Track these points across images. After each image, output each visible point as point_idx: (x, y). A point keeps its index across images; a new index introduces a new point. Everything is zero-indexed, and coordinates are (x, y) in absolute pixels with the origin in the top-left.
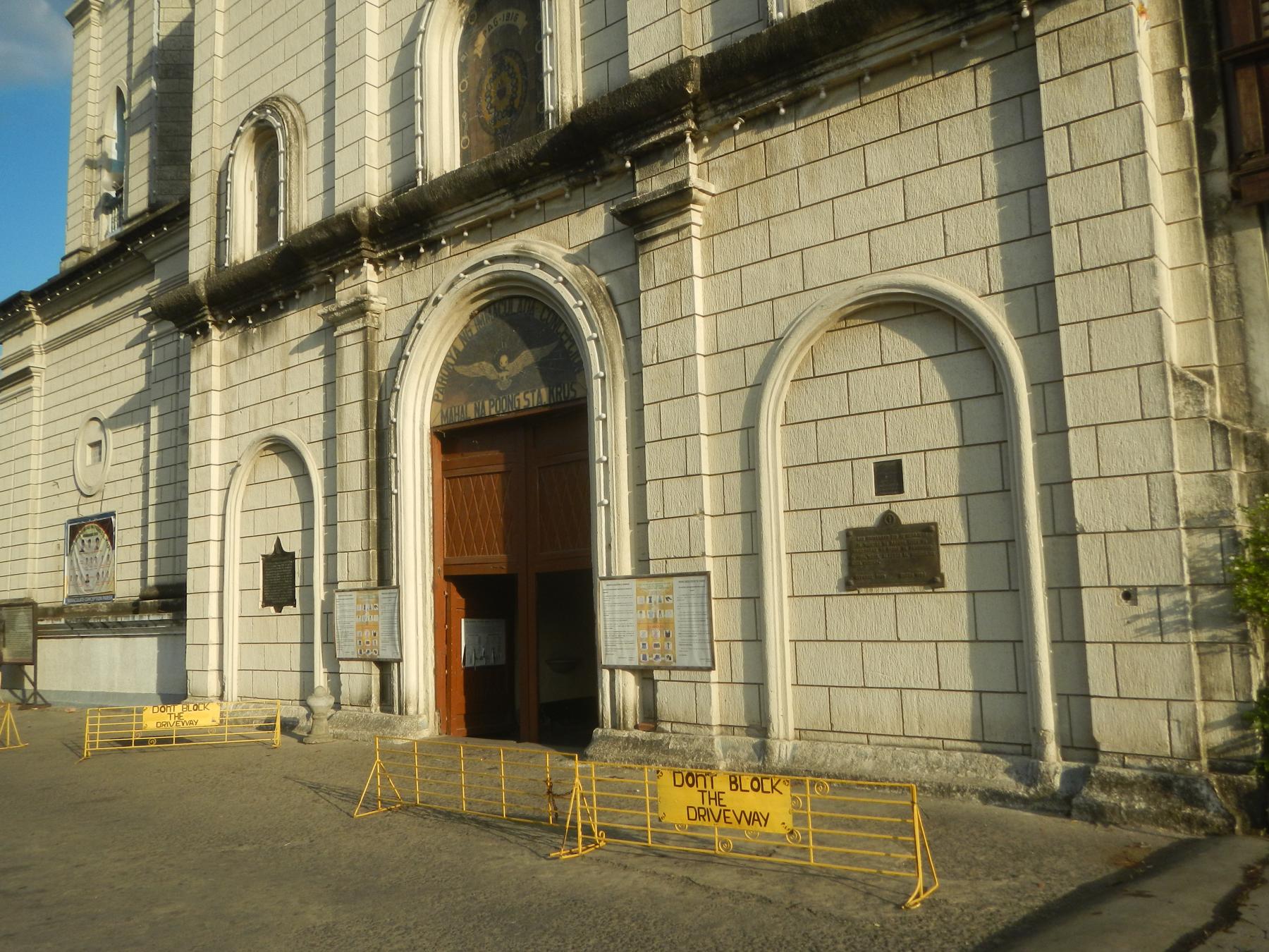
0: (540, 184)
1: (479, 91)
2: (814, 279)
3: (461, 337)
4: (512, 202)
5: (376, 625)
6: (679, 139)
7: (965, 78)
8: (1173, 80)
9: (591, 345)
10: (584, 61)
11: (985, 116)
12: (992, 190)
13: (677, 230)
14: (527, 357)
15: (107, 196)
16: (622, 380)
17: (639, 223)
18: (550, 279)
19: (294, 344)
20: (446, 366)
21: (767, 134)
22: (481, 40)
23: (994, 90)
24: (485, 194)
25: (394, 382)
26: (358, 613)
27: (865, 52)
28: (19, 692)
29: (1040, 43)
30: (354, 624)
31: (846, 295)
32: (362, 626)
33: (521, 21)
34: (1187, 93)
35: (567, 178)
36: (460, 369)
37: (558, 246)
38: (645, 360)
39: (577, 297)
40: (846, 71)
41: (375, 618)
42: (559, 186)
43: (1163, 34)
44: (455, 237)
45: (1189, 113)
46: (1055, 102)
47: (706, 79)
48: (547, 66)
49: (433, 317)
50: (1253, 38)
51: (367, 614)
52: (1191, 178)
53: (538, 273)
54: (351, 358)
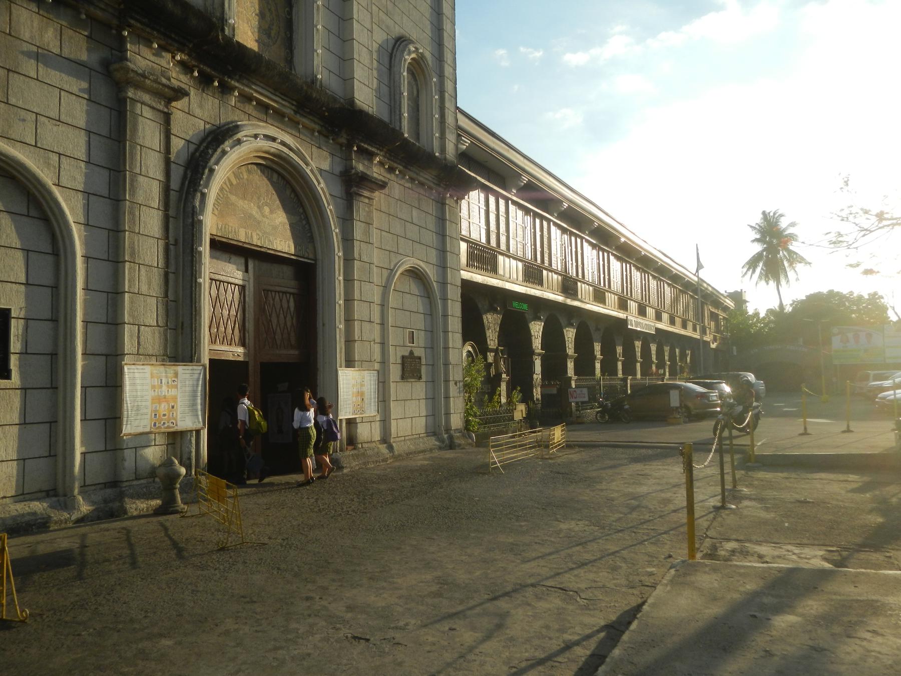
0: (311, 117)
4: (292, 113)
5: (175, 398)
13: (369, 198)
19: (35, 49)
24: (285, 95)
26: (153, 387)
27: (421, 174)
28: (591, 413)
30: (149, 398)
32: (158, 400)
35: (322, 126)
41: (173, 392)
42: (317, 127)
44: (246, 98)
51: (164, 388)
54: (147, 131)
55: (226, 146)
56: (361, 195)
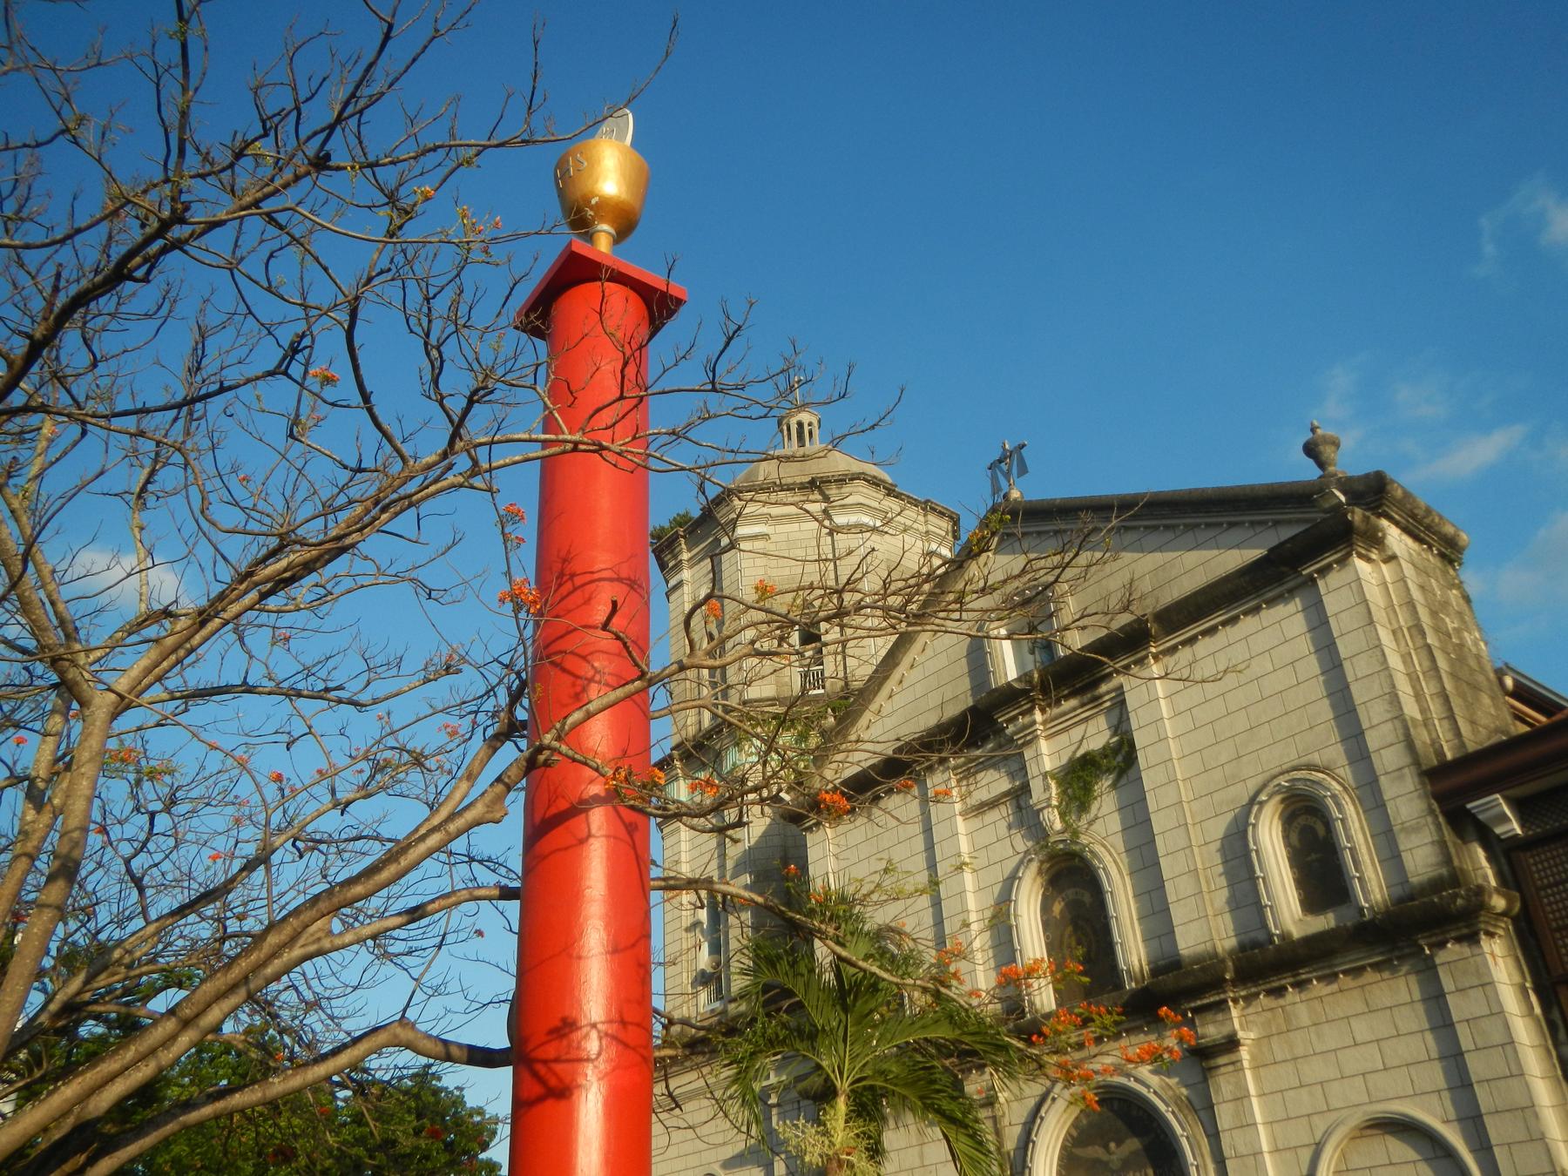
1: (1061, 943)
2: (1335, 1104)
3: (1075, 1125)
6: (1225, 1001)
7: (1401, 982)
8: (1524, 990)
9: (1184, 1142)
10: (1143, 932)
11: (1420, 1008)
12: (1434, 1055)
13: (1233, 1063)
14: (1133, 1144)
15: (703, 971)
16: (1211, 1167)
17: (1206, 1058)
18: (1144, 1090)
20: (1064, 1148)
21: (1281, 1002)
22: (1057, 908)
23: (1422, 992)
25: (1024, 1161)
29: (1441, 970)
31: (1357, 1118)
33: (1087, 898)
34: (1533, 998)
36: (1079, 1152)
37: (1142, 1068)
38: (1227, 1154)
39: (1167, 1105)
40: (1327, 971)
42: (1138, 1023)
43: (1510, 961)
45: (1538, 1010)
46: (1458, 1007)
47: (1237, 970)
48: (1117, 938)
49: (1052, 1112)
50: (1561, 971)
52: (1548, 1051)
53: (1132, 1084)
55: (1042, 1113)
56: (1218, 1067)
